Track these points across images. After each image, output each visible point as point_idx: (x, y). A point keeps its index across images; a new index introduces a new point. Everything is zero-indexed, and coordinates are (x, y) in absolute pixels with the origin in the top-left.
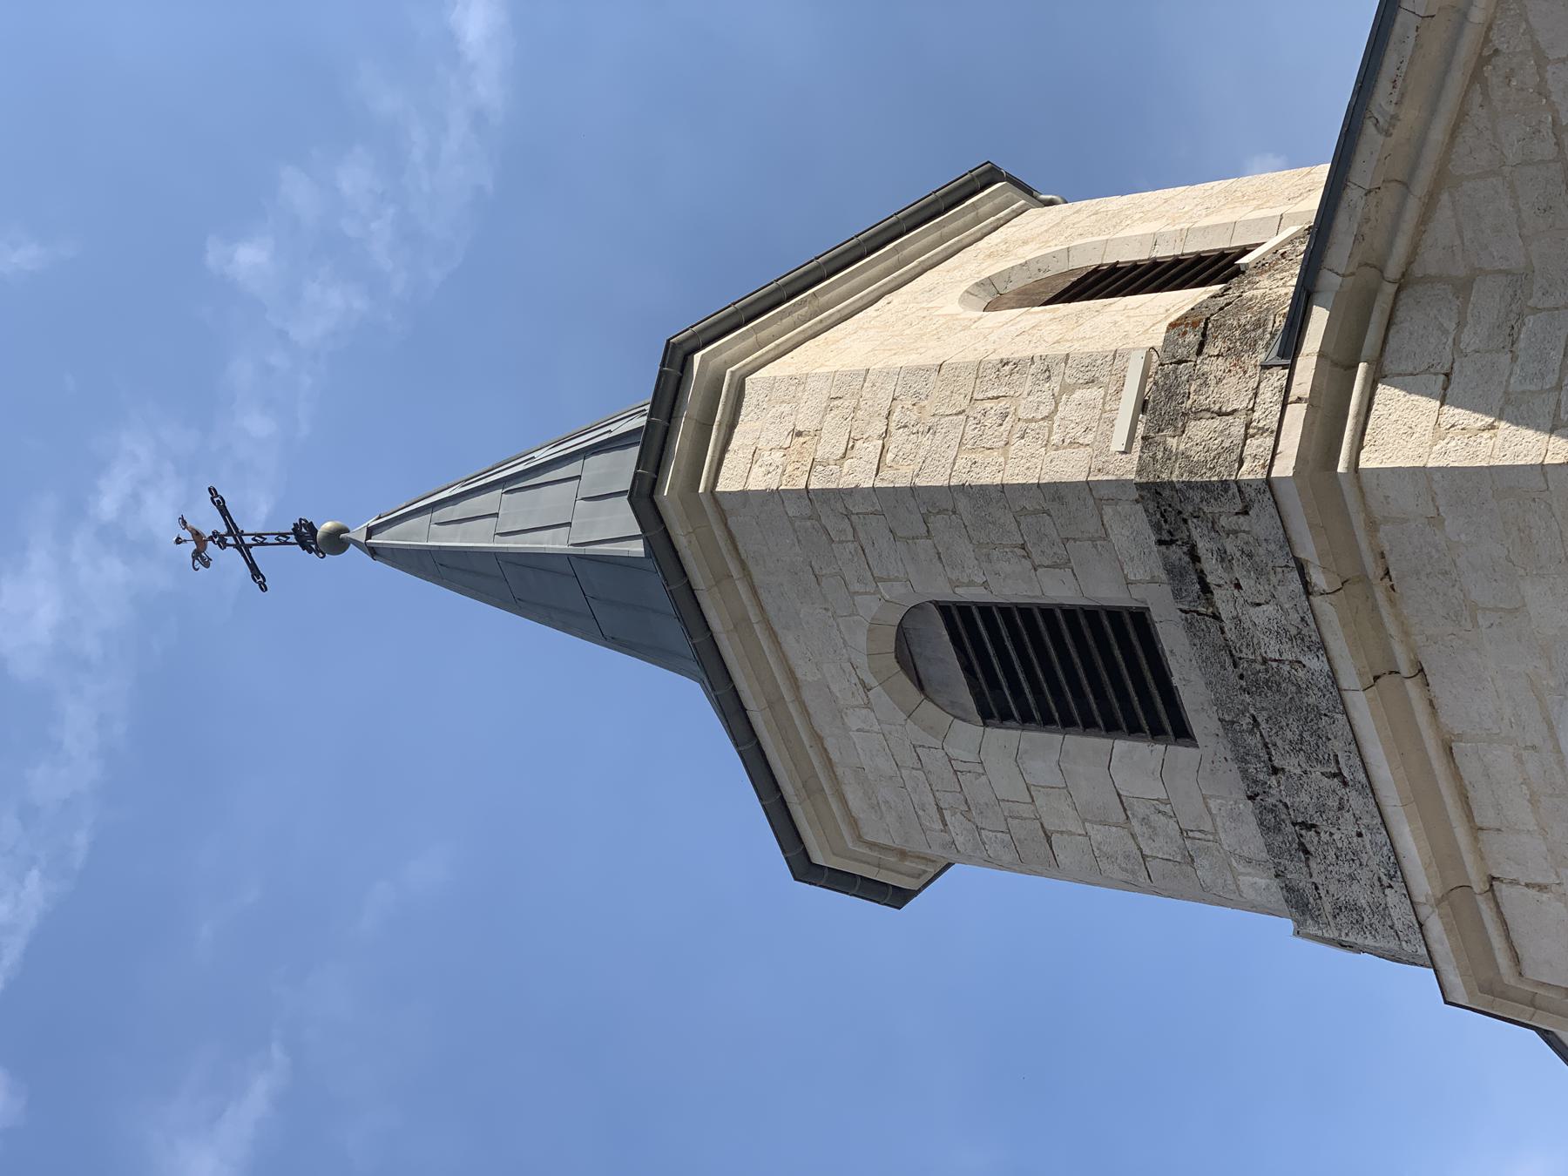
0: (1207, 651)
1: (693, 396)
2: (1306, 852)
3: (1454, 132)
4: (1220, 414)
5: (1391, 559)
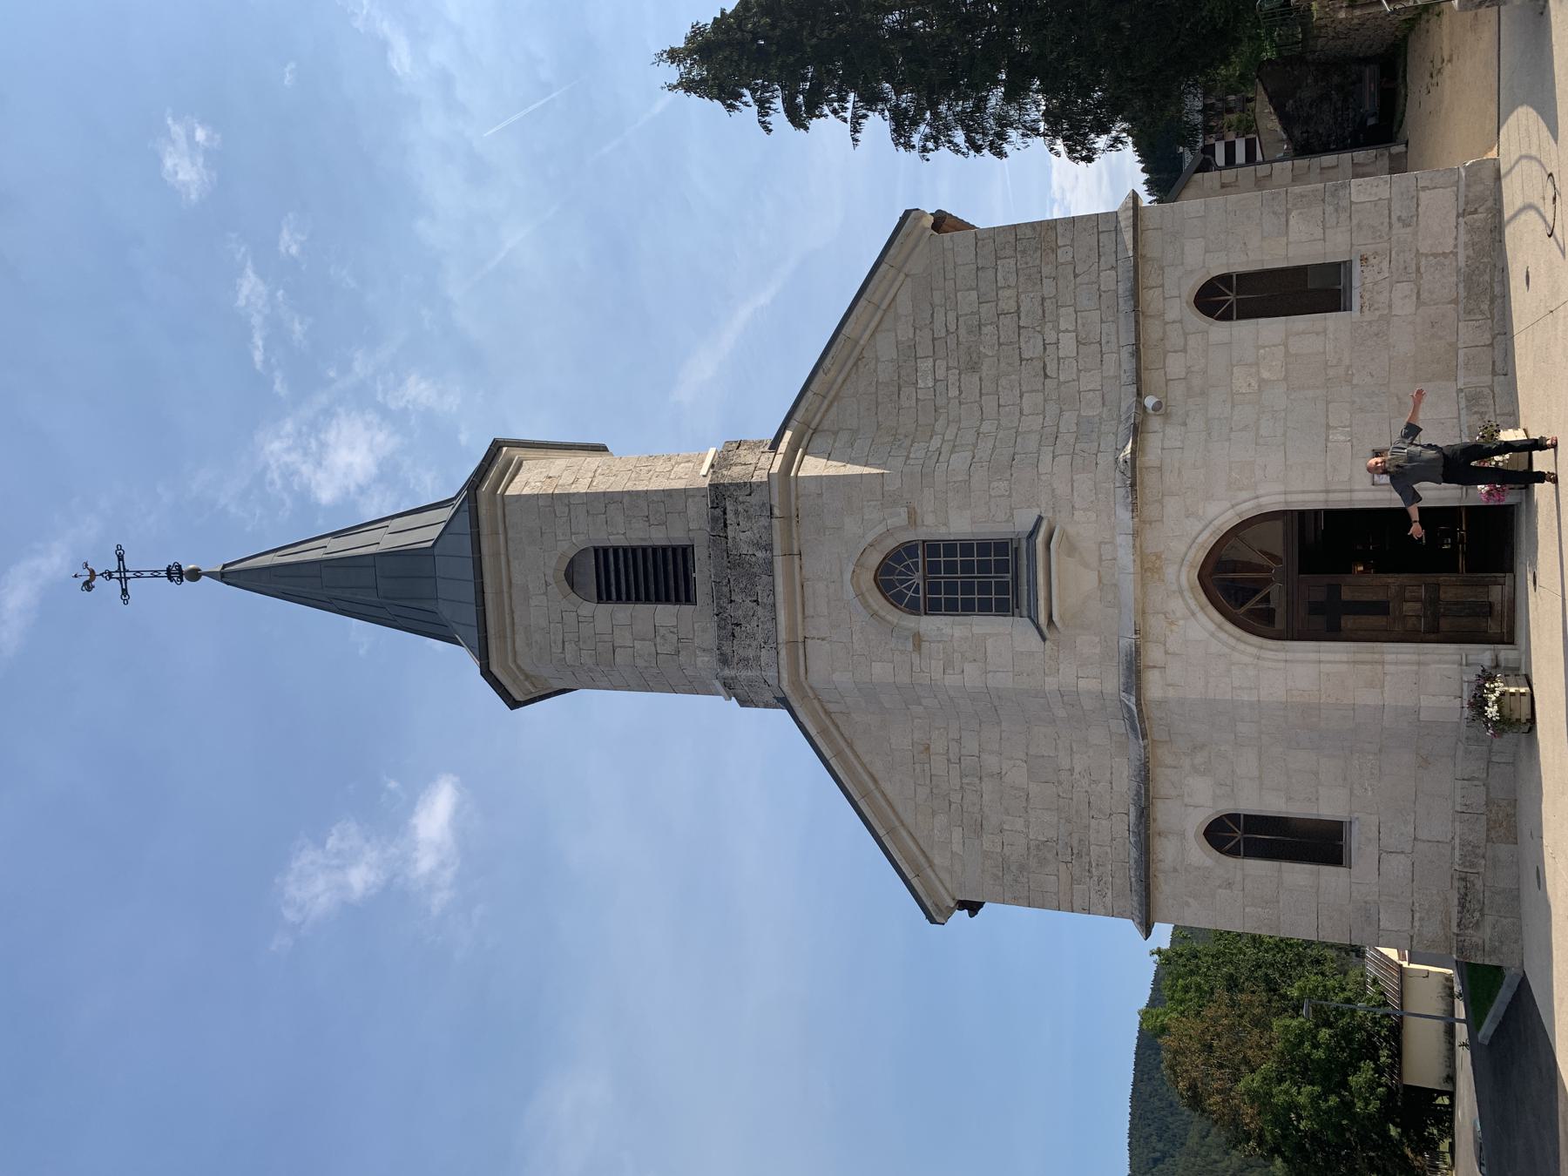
1: (501, 460)
2: (734, 636)
3: (844, 381)
4: (745, 464)
5: (800, 511)
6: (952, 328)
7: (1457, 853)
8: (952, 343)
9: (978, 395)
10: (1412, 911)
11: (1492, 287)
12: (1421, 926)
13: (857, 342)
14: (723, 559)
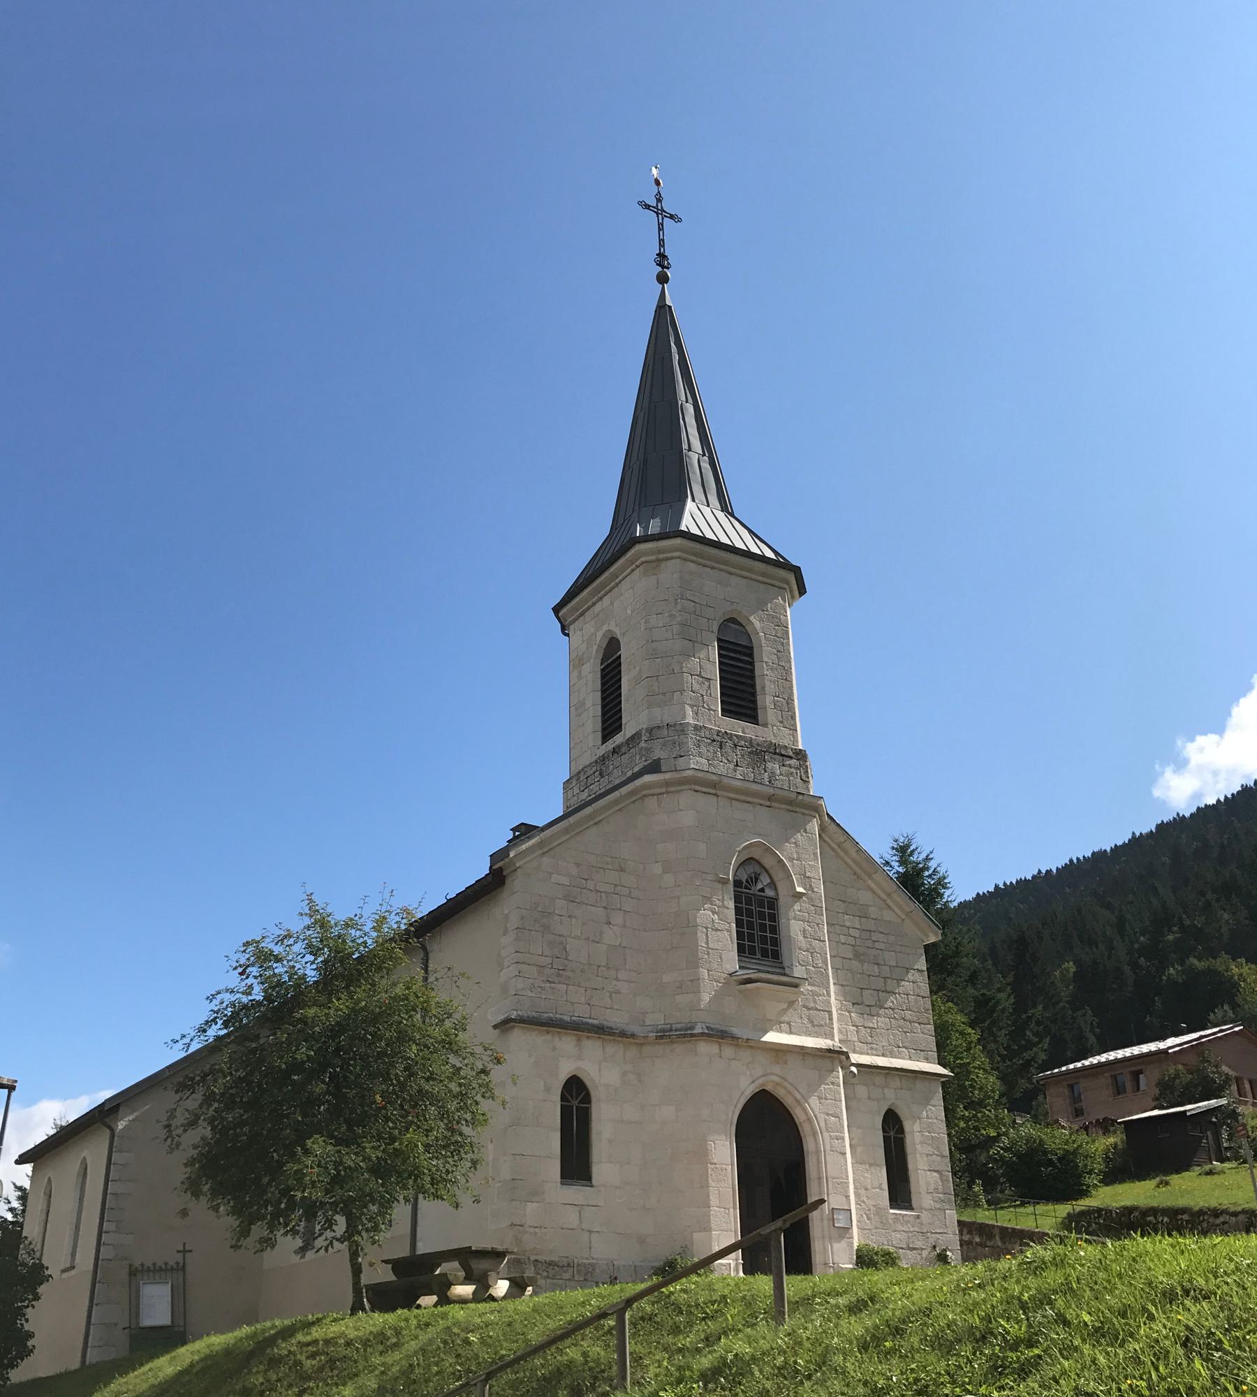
3: (846, 863)
6: (876, 945)
7: (585, 1261)
12: (531, 1233)
13: (870, 876)
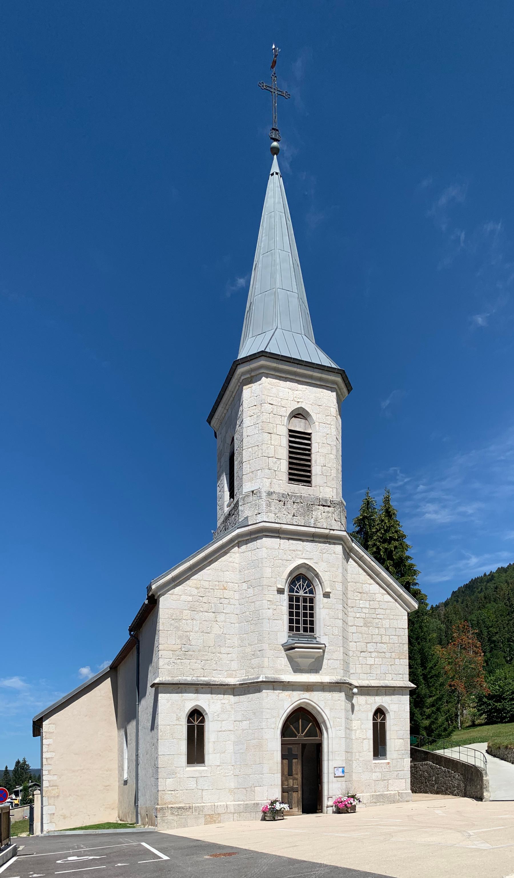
0: (314, 500)
2: (280, 501)
8: (374, 616)
9: (356, 625)
10: (175, 790)
11: (379, 802)
12: (169, 794)
14: (311, 502)
